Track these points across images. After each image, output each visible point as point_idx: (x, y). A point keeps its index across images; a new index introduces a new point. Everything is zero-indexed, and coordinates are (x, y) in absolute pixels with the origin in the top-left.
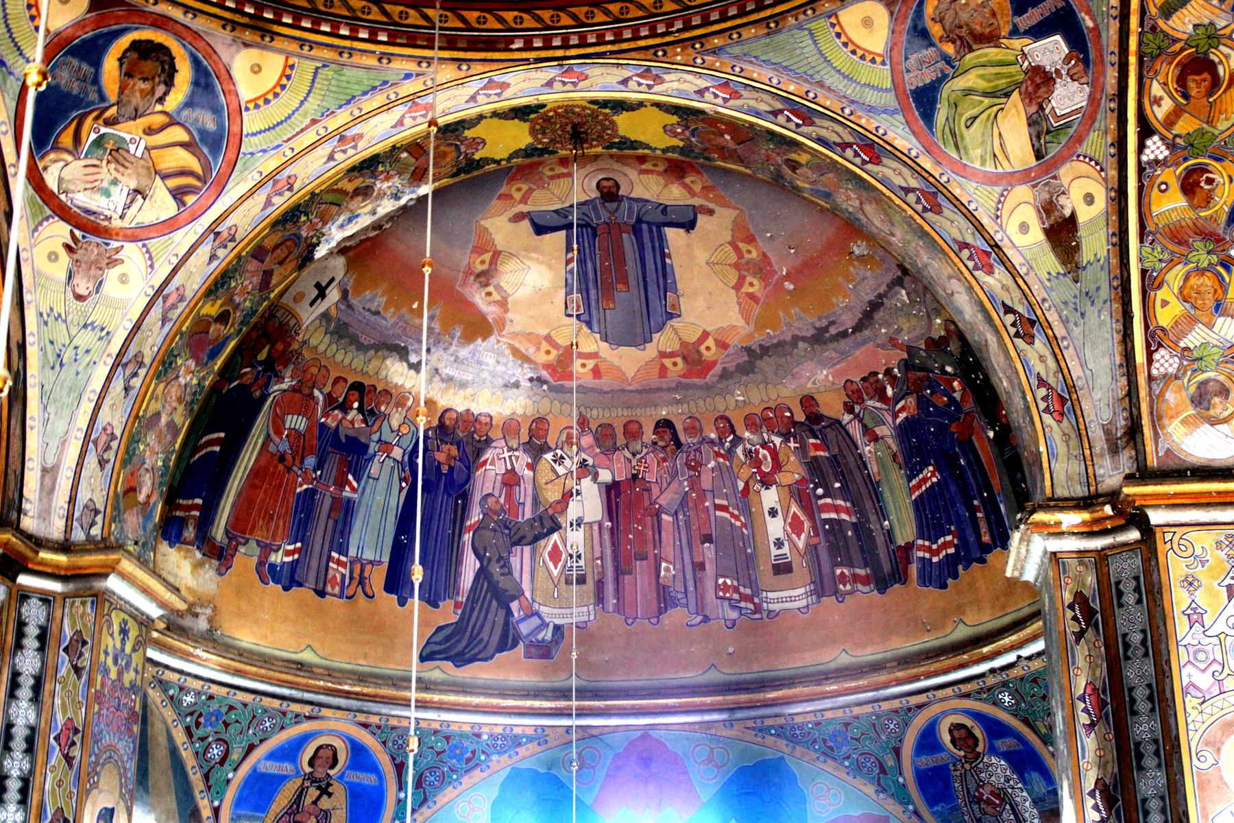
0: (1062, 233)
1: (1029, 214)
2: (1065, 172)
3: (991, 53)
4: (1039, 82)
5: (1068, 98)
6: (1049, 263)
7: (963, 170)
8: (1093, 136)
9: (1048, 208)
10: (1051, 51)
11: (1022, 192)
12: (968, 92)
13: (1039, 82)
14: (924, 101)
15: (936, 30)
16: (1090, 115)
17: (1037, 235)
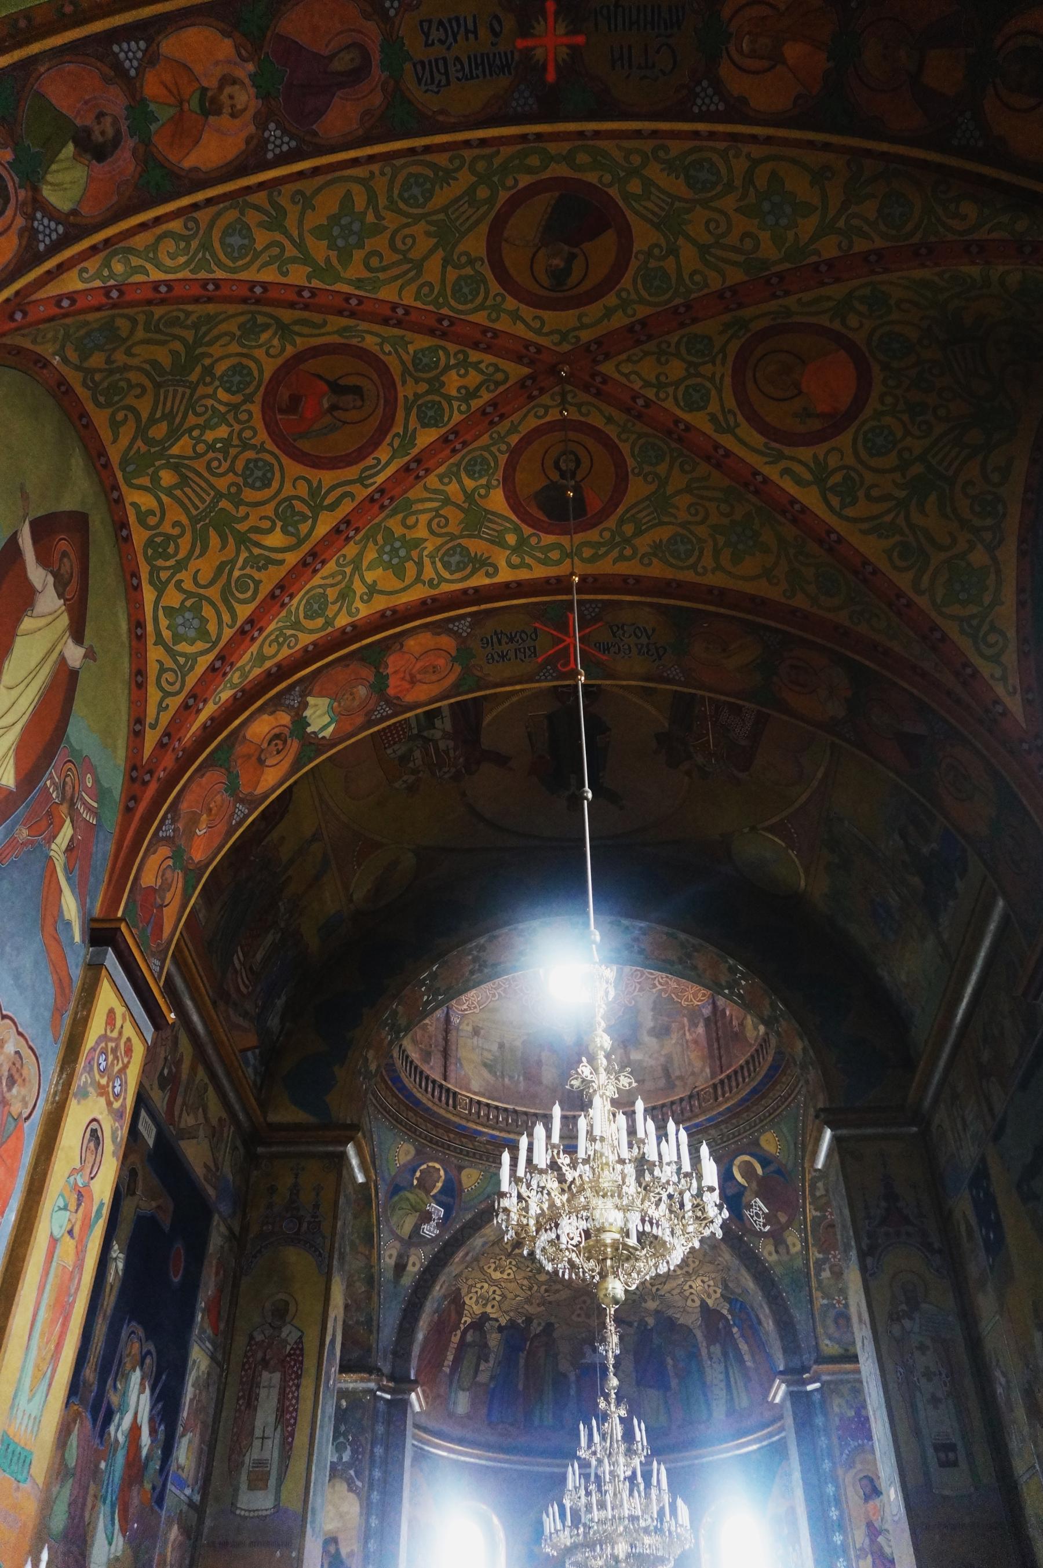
0: (400, 1268)
1: (395, 1253)
2: (413, 1250)
3: (423, 1195)
4: (427, 1217)
5: (429, 1230)
6: (390, 1275)
7: (388, 1221)
8: (429, 1247)
9: (400, 1256)
10: (438, 1211)
11: (398, 1244)
12: (408, 1199)
13: (427, 1217)
14: (396, 1189)
15: (418, 1174)
16: (433, 1240)
17: (392, 1262)
